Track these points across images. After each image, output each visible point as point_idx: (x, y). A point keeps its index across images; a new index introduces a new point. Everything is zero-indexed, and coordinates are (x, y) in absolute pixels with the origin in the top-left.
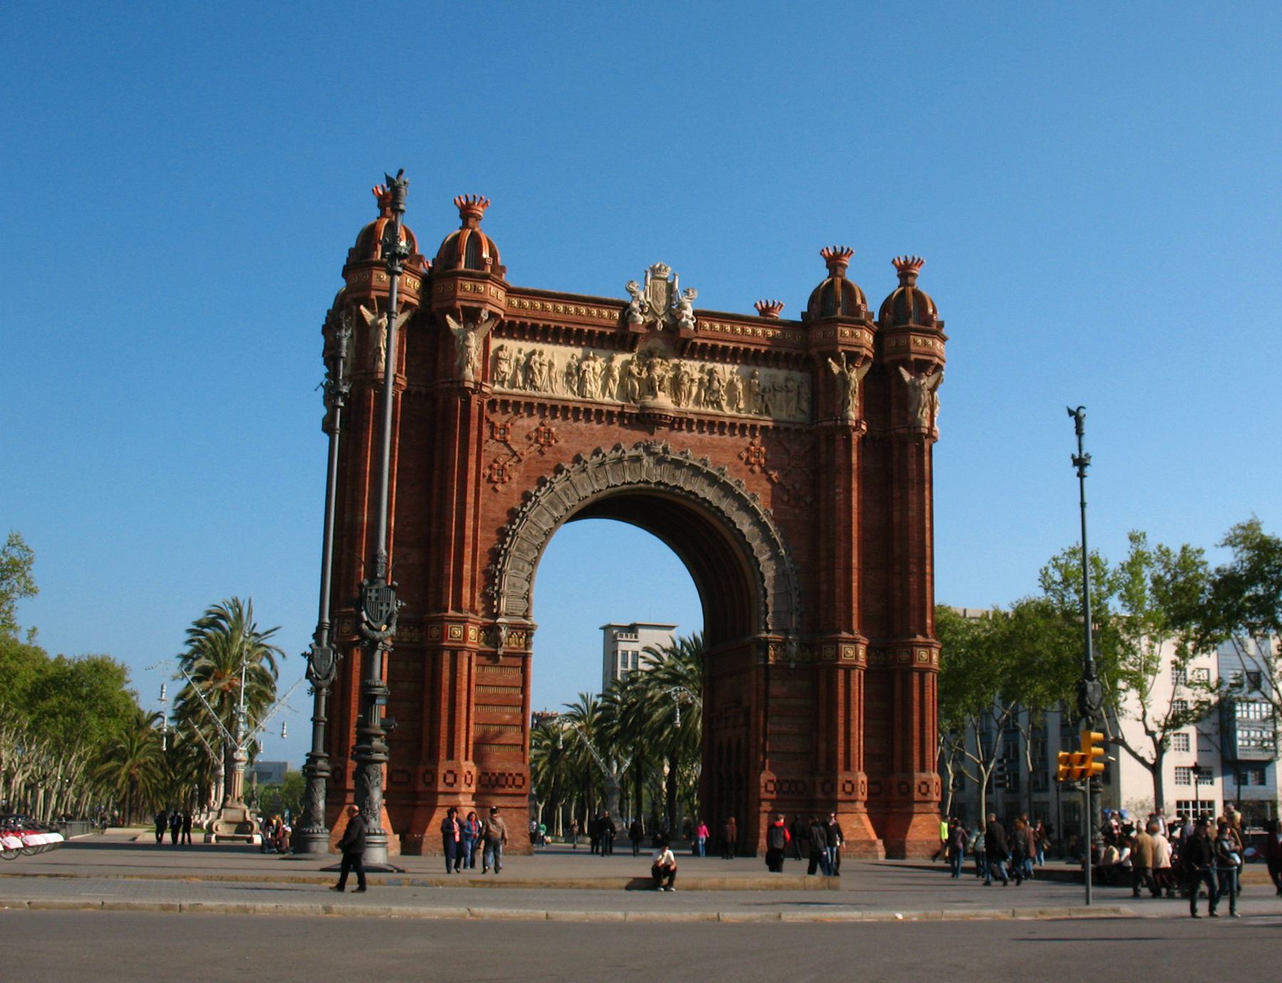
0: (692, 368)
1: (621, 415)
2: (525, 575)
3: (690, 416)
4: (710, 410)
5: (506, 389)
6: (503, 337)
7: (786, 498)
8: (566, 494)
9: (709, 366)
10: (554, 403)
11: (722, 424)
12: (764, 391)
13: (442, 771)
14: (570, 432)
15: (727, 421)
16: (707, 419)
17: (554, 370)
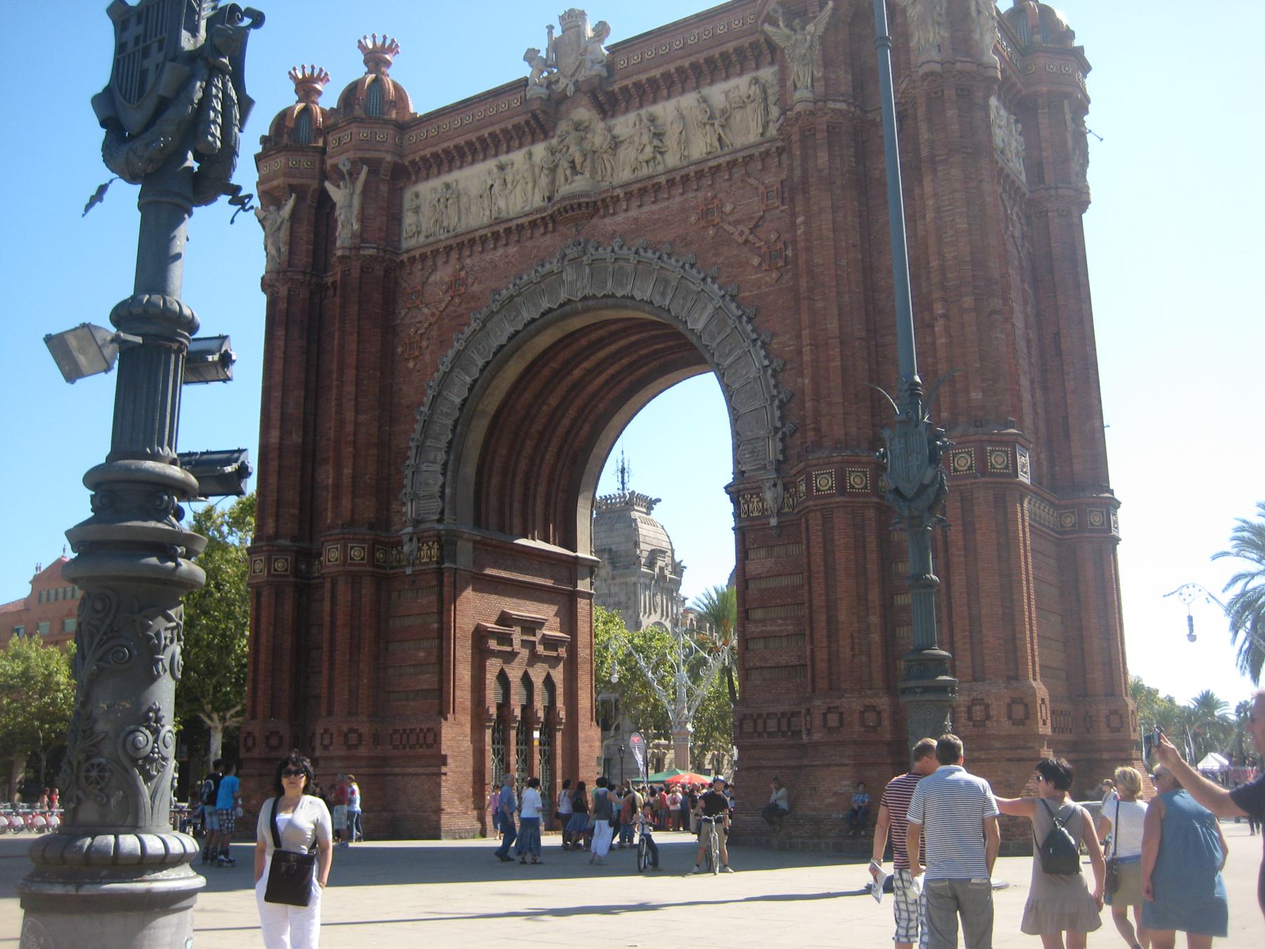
0: (624, 124)
1: (533, 224)
2: (438, 468)
3: (618, 191)
4: (645, 171)
5: (422, 239)
6: (416, 182)
7: (756, 261)
8: (478, 350)
9: (643, 112)
10: (459, 240)
11: (657, 188)
12: (712, 117)
13: (319, 731)
14: (484, 270)
15: (663, 179)
16: (635, 187)
17: (464, 200)
